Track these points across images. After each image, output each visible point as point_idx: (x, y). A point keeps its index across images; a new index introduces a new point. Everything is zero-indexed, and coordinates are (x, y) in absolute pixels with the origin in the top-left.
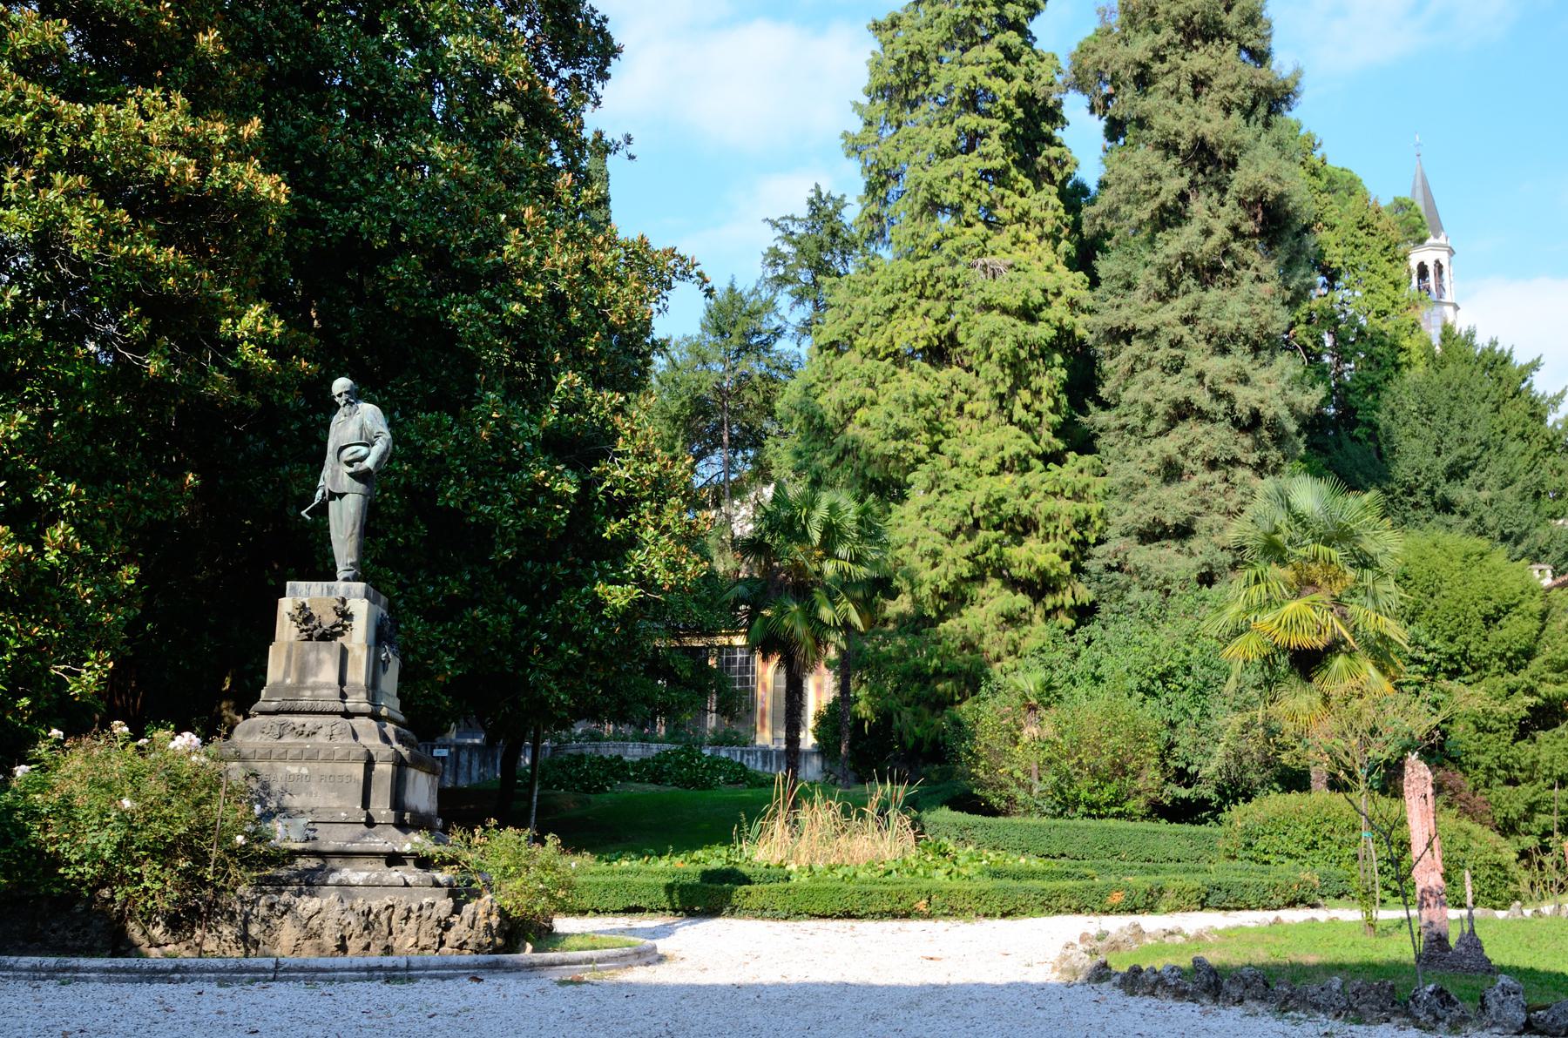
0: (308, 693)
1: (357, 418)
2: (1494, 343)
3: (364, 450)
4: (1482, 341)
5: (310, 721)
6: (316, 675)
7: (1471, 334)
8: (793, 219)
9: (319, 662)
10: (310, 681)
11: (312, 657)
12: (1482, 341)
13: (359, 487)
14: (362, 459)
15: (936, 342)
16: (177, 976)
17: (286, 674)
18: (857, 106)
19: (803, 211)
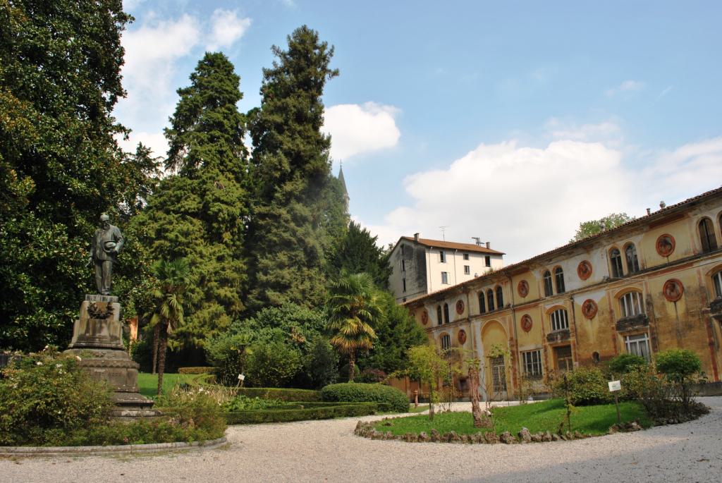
0: (97, 340)
1: (110, 231)
2: (365, 230)
3: (114, 244)
4: (361, 229)
5: (100, 351)
6: (100, 333)
7: (359, 226)
8: (130, 154)
9: (101, 328)
10: (97, 335)
11: (98, 325)
12: (361, 229)
13: (110, 258)
14: (114, 247)
15: (196, 210)
16: (93, 453)
17: (87, 331)
18: (171, 119)
19: (135, 152)
